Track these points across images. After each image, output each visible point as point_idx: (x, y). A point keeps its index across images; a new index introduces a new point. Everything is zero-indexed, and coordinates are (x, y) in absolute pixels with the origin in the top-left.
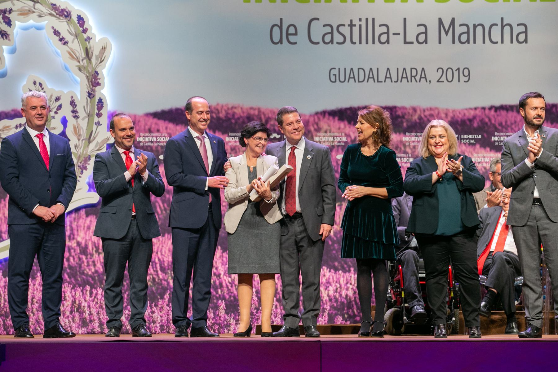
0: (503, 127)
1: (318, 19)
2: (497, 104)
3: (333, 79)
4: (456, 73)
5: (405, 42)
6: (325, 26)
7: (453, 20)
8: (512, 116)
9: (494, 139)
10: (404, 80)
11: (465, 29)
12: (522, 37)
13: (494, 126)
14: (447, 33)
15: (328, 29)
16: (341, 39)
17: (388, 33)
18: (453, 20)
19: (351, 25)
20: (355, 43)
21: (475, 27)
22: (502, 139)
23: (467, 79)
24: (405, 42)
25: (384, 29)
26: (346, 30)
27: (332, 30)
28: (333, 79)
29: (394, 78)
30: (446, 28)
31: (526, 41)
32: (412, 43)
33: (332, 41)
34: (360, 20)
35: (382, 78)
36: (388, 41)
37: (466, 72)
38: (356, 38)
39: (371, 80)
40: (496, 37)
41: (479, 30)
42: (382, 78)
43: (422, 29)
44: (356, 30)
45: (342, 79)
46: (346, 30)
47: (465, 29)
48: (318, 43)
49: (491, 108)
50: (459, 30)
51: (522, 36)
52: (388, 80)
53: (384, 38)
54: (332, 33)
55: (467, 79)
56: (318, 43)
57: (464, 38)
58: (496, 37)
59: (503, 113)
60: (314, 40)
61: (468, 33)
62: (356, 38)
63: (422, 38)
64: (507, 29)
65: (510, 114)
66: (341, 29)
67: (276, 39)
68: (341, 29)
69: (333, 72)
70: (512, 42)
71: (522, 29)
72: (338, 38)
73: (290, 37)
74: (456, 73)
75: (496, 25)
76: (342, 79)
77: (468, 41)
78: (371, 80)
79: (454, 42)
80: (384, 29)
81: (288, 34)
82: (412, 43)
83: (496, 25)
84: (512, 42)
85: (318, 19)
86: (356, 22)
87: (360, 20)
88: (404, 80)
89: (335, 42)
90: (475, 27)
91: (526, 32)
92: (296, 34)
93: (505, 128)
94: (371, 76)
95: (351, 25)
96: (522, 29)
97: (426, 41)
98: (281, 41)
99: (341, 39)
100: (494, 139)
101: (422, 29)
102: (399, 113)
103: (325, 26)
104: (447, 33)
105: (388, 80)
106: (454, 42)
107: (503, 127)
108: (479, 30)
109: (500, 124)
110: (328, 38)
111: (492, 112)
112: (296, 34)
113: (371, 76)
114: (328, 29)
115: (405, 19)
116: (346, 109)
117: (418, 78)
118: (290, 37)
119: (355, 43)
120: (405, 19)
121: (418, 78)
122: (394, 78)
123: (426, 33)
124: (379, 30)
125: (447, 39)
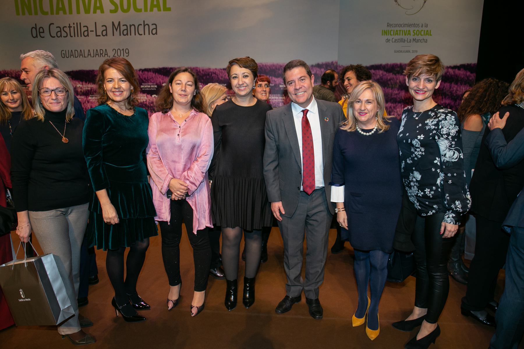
0: (146, 80)
1: (53, 24)
2: (143, 68)
3: (63, 56)
4: (122, 52)
5: (97, 36)
6: (57, 27)
7: (119, 22)
8: (151, 74)
9: (142, 86)
10: (97, 56)
11: (125, 27)
12: (154, 31)
13: (142, 79)
14: (117, 30)
15: (59, 29)
16: (65, 35)
17: (88, 30)
18: (119, 22)
19: (70, 27)
20: (72, 37)
21: (130, 26)
22: (146, 87)
23: (127, 55)
24: (97, 36)
25: (86, 29)
26: (67, 29)
27: (61, 29)
28: (63, 56)
29: (92, 55)
30: (116, 27)
31: (156, 33)
32: (100, 36)
33: (61, 36)
34: (74, 24)
35: (86, 55)
36: (88, 35)
37: (127, 52)
38: (72, 34)
39: (81, 56)
40: (141, 31)
41: (133, 27)
42: (86, 55)
43: (104, 28)
44: (72, 29)
45: (67, 56)
46: (67, 29)
47: (125, 27)
48: (54, 37)
49: (140, 70)
50: (123, 28)
51: (154, 30)
52: (89, 56)
53: (86, 34)
54: (61, 31)
55: (127, 55)
56: (54, 37)
57: (125, 32)
58: (141, 32)
59: (146, 73)
60: (53, 35)
61: (127, 29)
62: (72, 34)
63: (104, 33)
64: (147, 27)
65: (150, 73)
66: (65, 29)
67: (35, 35)
68: (65, 29)
69: (63, 52)
70: (149, 34)
71: (154, 26)
72: (64, 34)
73: (41, 34)
74: (122, 52)
75: (141, 25)
76: (67, 56)
77: (127, 34)
78: (81, 56)
79: (120, 35)
80: (86, 29)
81: (40, 32)
82: (100, 36)
83: (141, 25)
84: (149, 34)
85: (53, 24)
86: (72, 25)
87: (74, 24)
88: (97, 56)
89: (62, 36)
90: (130, 26)
91: (156, 29)
92: (43, 32)
93: (147, 81)
94: (81, 54)
95: (70, 27)
96: (154, 26)
97: (106, 35)
98: (37, 36)
99: (65, 35)
100: (142, 86)
101: (104, 28)
102: (96, 73)
103: (57, 27)
104: (117, 30)
105: (89, 56)
106: (120, 35)
107: (146, 80)
108: (133, 27)
109: (145, 79)
110: (59, 34)
111: (141, 72)
112: (43, 32)
113: (81, 54)
114: (59, 29)
115: (96, 23)
116: (71, 72)
117: (103, 55)
118: (41, 34)
119: (72, 37)
120: (96, 23)
121: (103, 55)
122: (92, 55)
123: (106, 30)
124: (84, 29)
125: (117, 33)
